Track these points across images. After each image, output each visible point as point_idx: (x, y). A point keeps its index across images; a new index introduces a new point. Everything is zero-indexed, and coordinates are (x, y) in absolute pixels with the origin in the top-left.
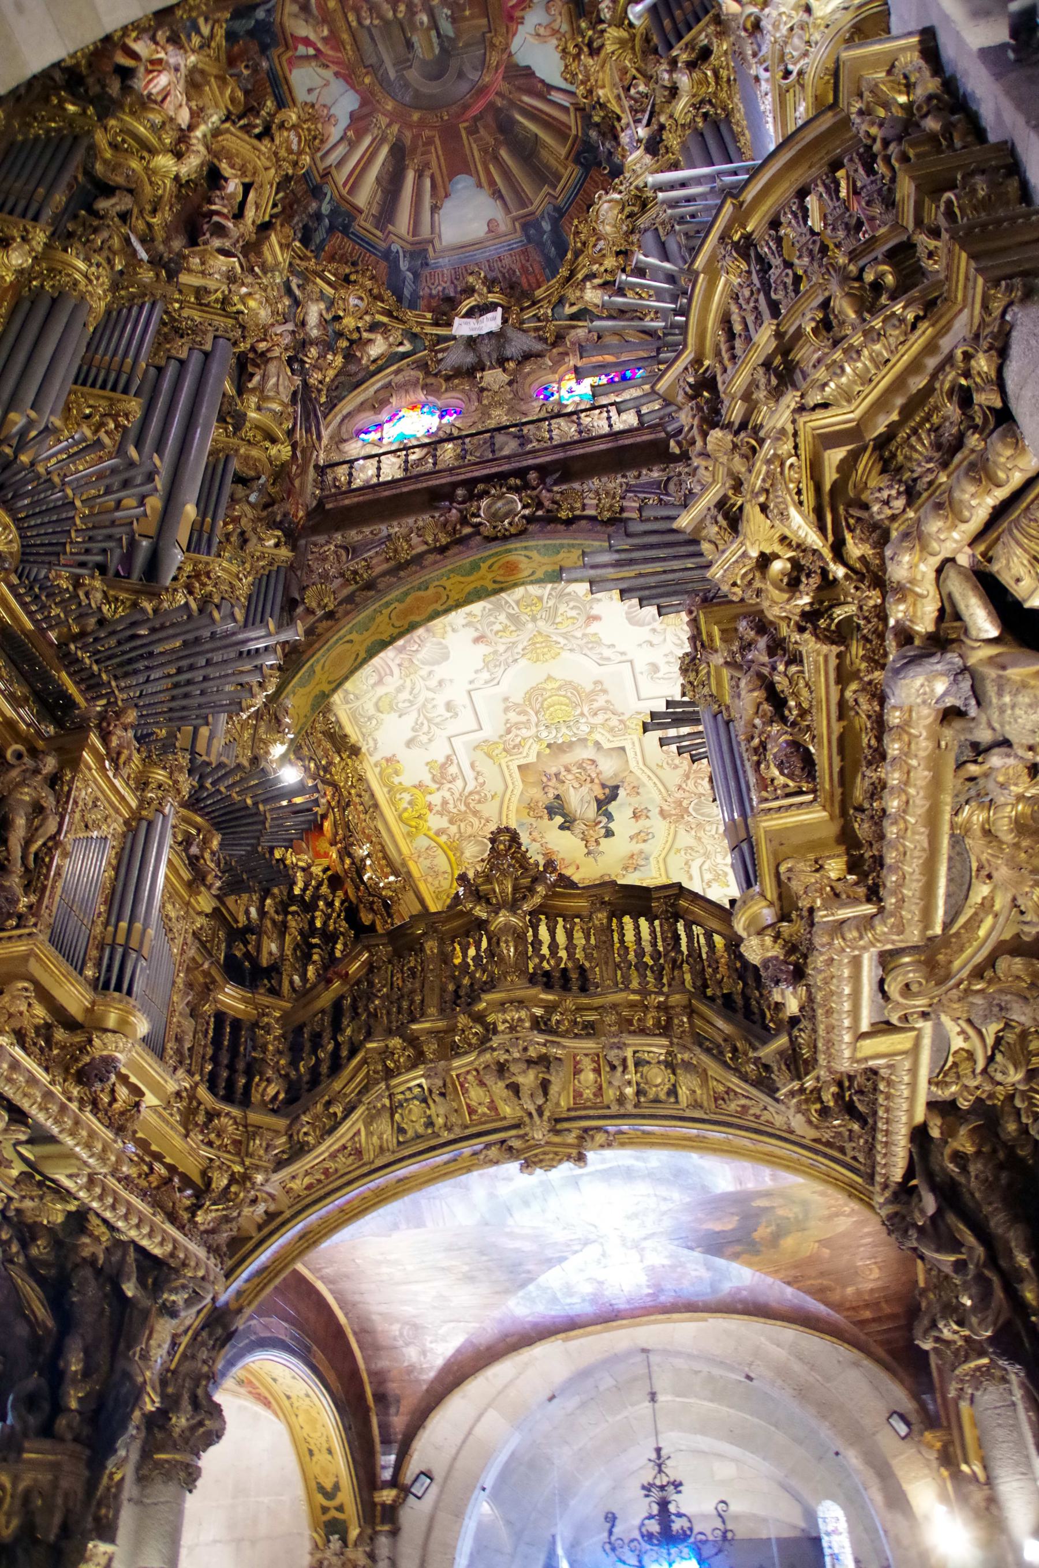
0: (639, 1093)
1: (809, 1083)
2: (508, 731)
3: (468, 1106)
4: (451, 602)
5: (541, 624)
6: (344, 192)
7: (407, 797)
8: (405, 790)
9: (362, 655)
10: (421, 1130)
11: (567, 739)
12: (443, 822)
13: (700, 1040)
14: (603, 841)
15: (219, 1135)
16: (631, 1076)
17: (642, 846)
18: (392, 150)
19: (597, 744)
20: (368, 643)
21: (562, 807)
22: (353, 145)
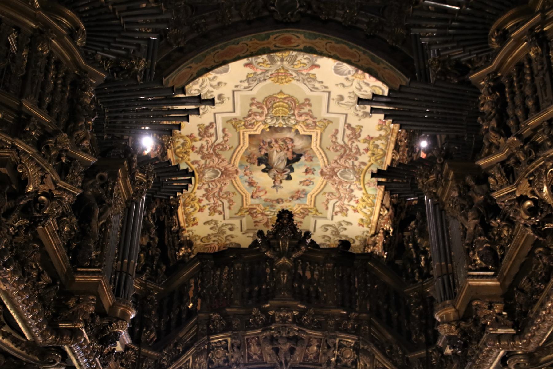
0: (337, 361)
2: (249, 116)
3: (248, 354)
4: (248, 53)
5: (285, 63)
7: (181, 141)
8: (182, 137)
9: (195, 75)
10: (221, 363)
11: (281, 126)
12: (198, 157)
13: (373, 340)
14: (284, 182)
15: (127, 360)
16: (336, 352)
17: (305, 187)
19: (297, 132)
20: (199, 69)
21: (267, 160)
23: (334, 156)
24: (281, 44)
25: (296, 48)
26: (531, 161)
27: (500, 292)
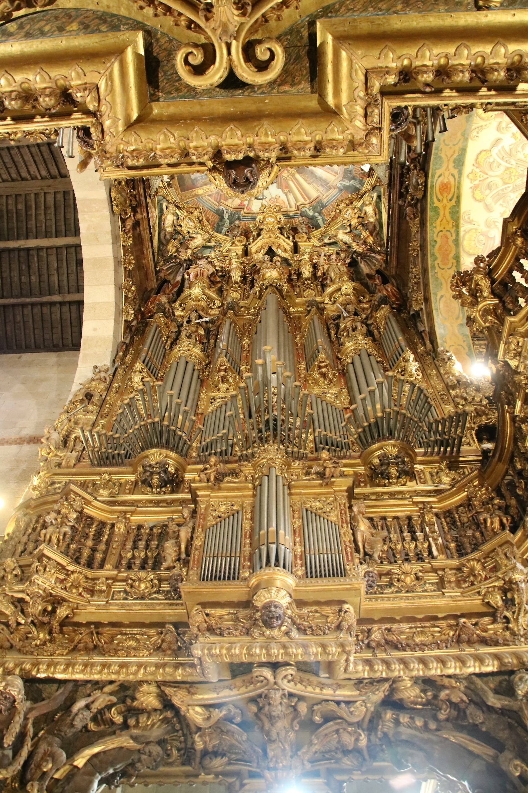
4: (453, 230)
6: (308, 201)
18: (299, 173)
22: (291, 191)
24: (448, 194)
25: (457, 177)
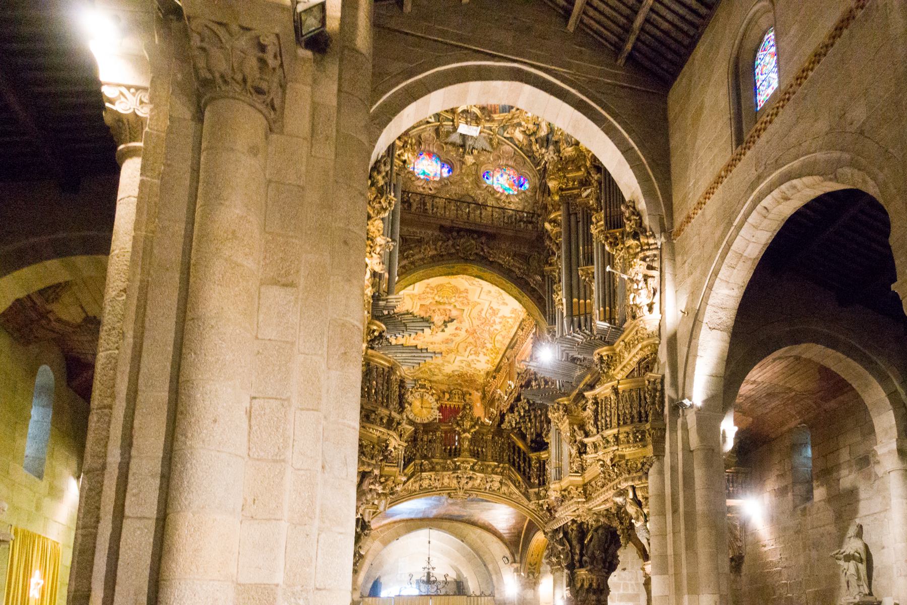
1: (541, 502)
23: (476, 322)
26: (605, 448)
27: (582, 483)
